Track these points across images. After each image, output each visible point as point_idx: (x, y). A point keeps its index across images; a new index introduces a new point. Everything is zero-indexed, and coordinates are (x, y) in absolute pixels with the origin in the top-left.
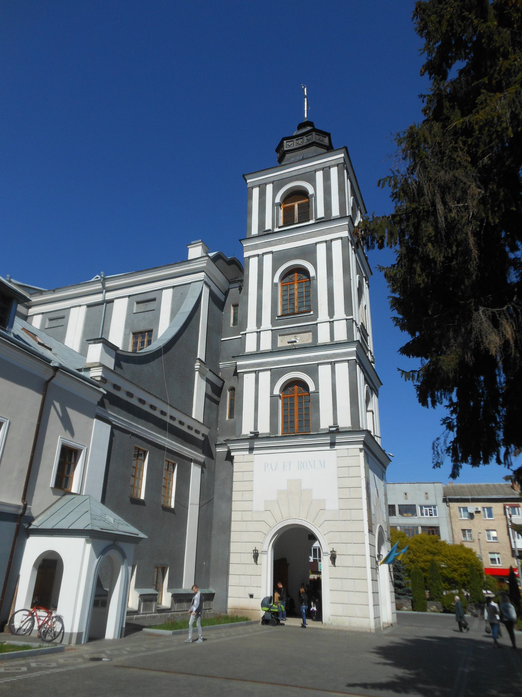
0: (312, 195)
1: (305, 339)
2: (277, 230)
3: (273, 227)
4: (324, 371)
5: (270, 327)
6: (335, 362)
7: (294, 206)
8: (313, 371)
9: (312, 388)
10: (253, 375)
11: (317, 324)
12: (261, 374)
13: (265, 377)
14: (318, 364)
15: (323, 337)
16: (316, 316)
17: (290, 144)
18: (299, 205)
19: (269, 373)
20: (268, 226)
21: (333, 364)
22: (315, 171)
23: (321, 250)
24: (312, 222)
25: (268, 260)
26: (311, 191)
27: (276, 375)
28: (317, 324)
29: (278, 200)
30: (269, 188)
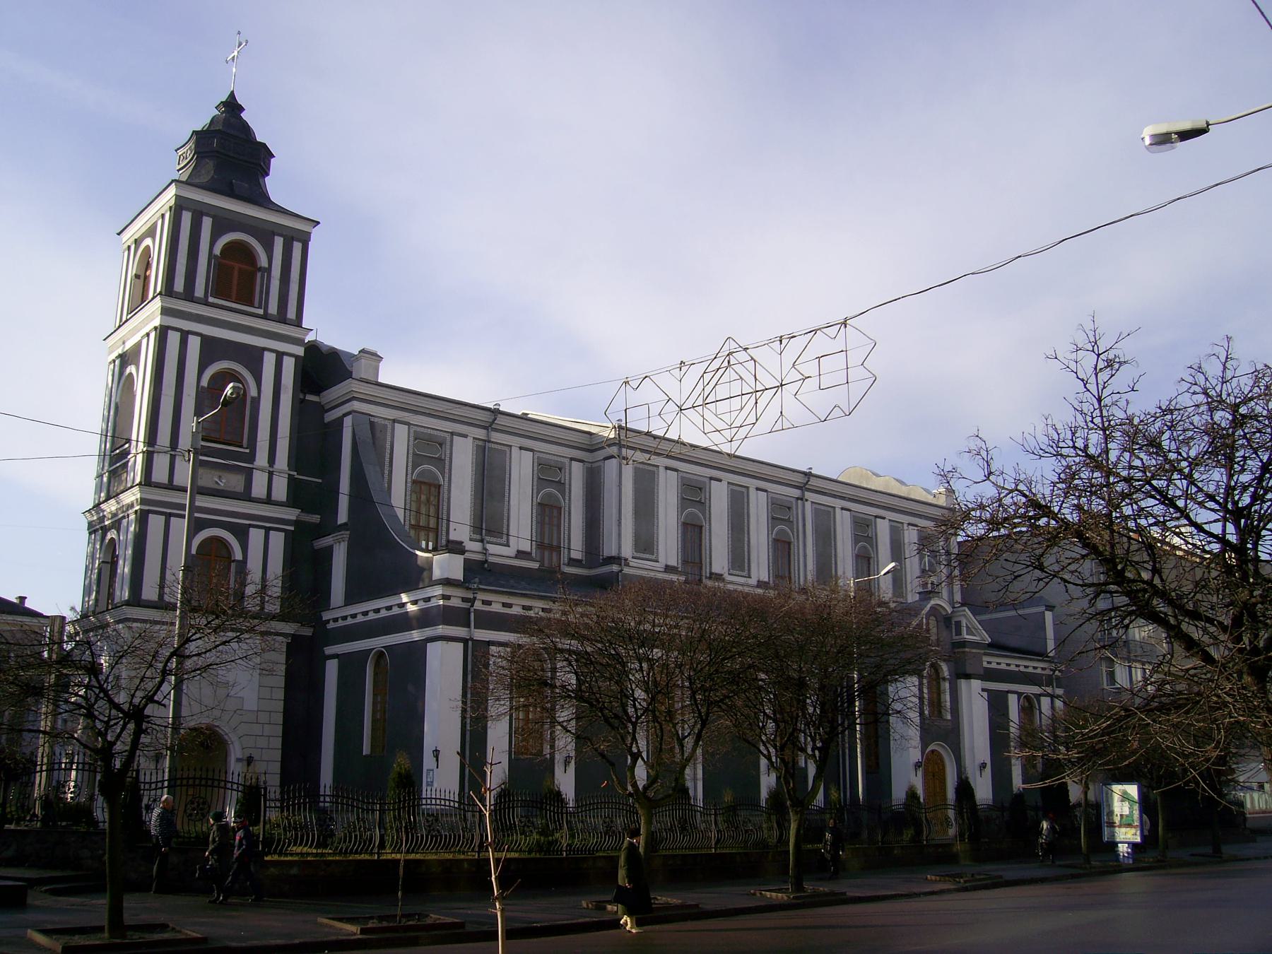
0: (264, 268)
1: (234, 482)
2: (211, 300)
4: (256, 536)
6: (271, 529)
8: (242, 533)
9: (238, 555)
10: (163, 518)
13: (181, 527)
14: (250, 526)
15: (259, 489)
16: (251, 457)
18: (240, 269)
20: (199, 291)
21: (268, 530)
22: (274, 234)
23: (269, 361)
24: (261, 312)
25: (194, 344)
26: (263, 262)
27: (196, 526)
29: (217, 250)
30: (207, 223)
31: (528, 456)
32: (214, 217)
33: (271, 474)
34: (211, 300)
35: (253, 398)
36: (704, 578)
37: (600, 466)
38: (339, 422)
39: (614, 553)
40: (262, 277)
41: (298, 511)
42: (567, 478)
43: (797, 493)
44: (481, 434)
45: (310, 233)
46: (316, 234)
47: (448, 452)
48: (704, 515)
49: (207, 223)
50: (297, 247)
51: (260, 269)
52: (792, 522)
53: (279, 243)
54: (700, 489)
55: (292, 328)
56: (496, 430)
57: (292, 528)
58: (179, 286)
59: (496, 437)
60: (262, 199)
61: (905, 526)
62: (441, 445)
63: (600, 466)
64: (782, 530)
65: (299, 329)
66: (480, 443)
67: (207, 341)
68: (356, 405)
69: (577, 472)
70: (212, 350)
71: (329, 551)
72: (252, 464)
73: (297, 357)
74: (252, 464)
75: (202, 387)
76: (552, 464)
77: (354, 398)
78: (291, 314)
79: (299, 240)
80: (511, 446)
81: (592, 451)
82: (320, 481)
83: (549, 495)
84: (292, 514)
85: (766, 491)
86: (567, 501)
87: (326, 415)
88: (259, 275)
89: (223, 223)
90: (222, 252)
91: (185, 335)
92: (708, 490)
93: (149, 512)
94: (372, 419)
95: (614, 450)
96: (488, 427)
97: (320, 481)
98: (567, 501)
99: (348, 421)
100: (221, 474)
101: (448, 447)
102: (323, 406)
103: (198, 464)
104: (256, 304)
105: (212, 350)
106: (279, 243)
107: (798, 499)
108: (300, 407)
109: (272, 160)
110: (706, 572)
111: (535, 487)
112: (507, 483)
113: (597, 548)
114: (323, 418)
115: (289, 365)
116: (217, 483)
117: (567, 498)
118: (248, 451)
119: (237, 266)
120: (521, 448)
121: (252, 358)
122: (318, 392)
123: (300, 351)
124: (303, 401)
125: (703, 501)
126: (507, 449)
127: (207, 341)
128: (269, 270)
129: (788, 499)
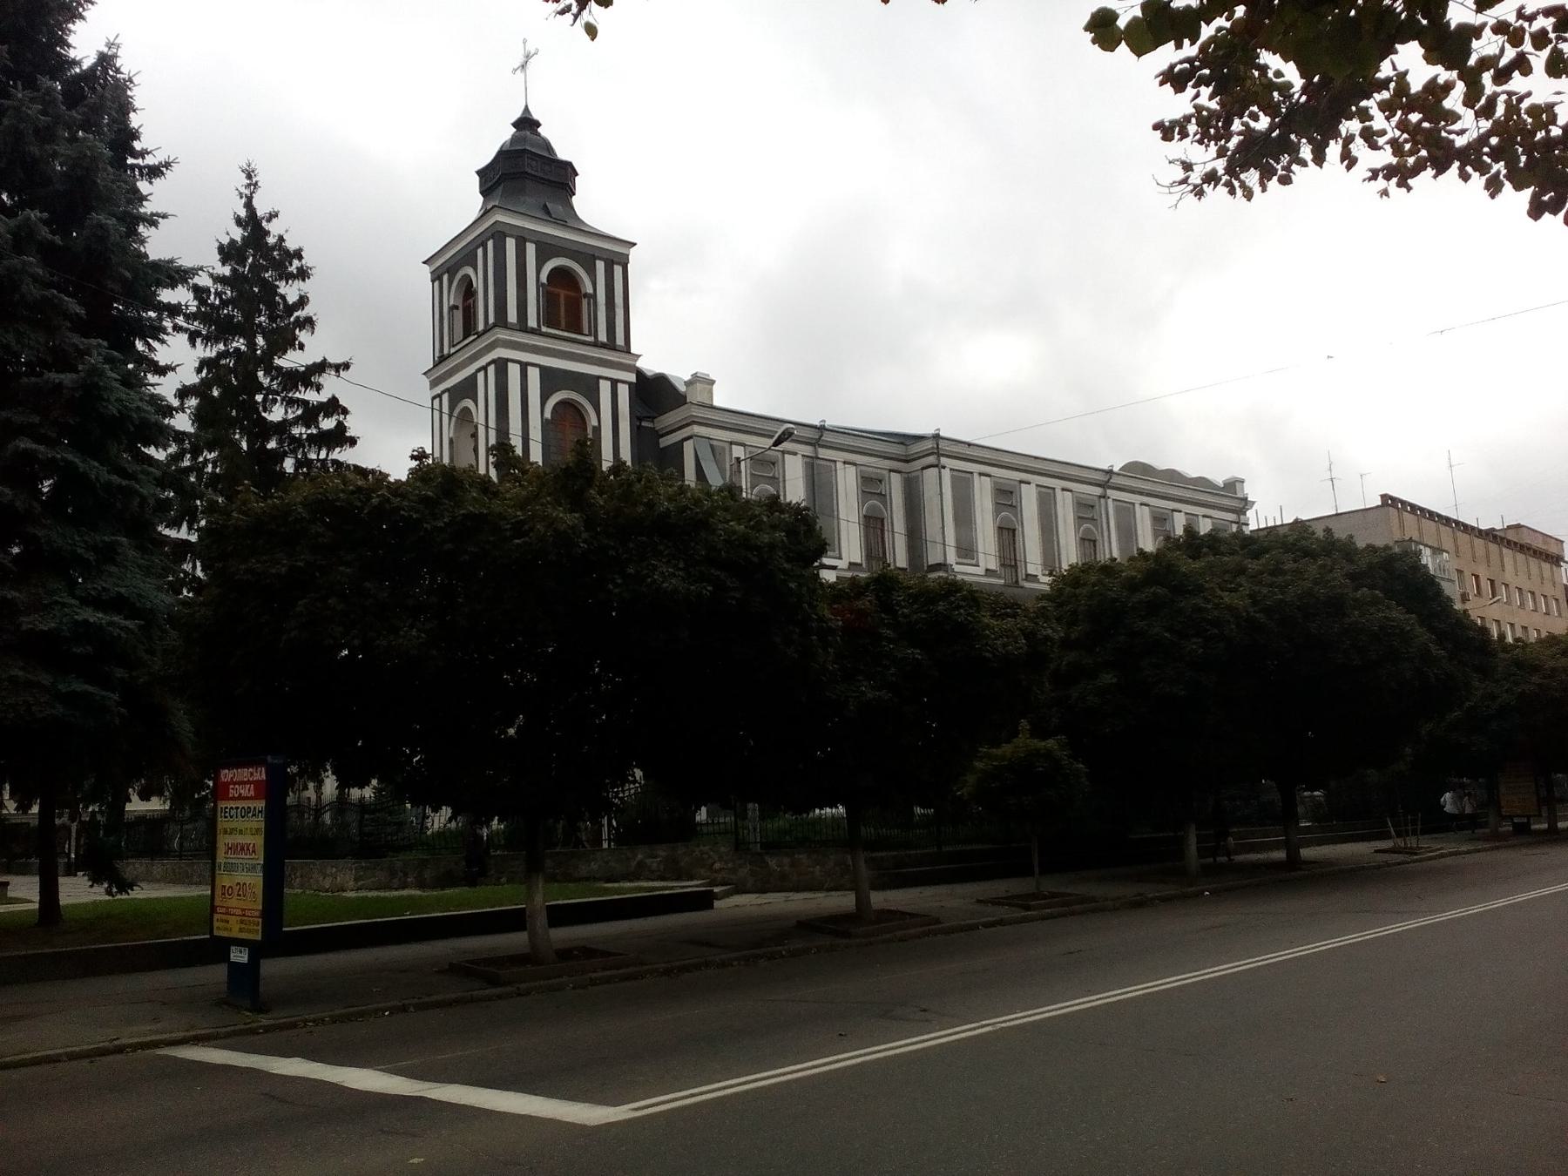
0: (589, 294)
2: (544, 329)
3: (539, 325)
7: (559, 295)
18: (567, 297)
23: (605, 387)
25: (534, 375)
29: (544, 278)
30: (531, 249)
31: (852, 469)
32: (536, 243)
34: (544, 329)
35: (594, 427)
36: (1020, 579)
37: (918, 477)
38: (679, 446)
39: (940, 560)
40: (589, 304)
42: (888, 490)
43: (1098, 491)
44: (808, 450)
45: (628, 255)
46: (633, 254)
47: (781, 471)
48: (1016, 516)
49: (531, 249)
50: (618, 270)
51: (586, 295)
52: (1096, 520)
53: (600, 265)
54: (1011, 493)
55: (623, 355)
56: (823, 446)
58: (512, 317)
59: (824, 453)
60: (569, 219)
61: (1137, 506)
62: (774, 464)
63: (918, 477)
64: (1089, 529)
65: (627, 356)
66: (808, 460)
67: (546, 372)
68: (697, 429)
69: (896, 482)
70: (552, 379)
73: (630, 384)
75: (547, 420)
76: (873, 476)
77: (694, 423)
79: (619, 264)
80: (835, 461)
81: (907, 461)
83: (873, 507)
85: (1071, 491)
86: (889, 512)
87: (661, 440)
88: (585, 302)
89: (547, 249)
90: (548, 281)
91: (524, 367)
92: (1018, 493)
94: (711, 442)
95: (931, 459)
96: (816, 443)
98: (889, 512)
99: (688, 447)
101: (781, 466)
102: (657, 431)
104: (586, 331)
105: (552, 379)
106: (600, 265)
107: (1100, 497)
108: (637, 432)
109: (577, 178)
110: (1022, 575)
111: (860, 501)
112: (835, 495)
113: (921, 557)
115: (624, 392)
117: (889, 509)
120: (845, 463)
121: (589, 386)
122: (652, 419)
123: (632, 378)
124: (639, 427)
125: (1014, 504)
126: (832, 465)
127: (546, 372)
128: (594, 296)
129: (1091, 497)
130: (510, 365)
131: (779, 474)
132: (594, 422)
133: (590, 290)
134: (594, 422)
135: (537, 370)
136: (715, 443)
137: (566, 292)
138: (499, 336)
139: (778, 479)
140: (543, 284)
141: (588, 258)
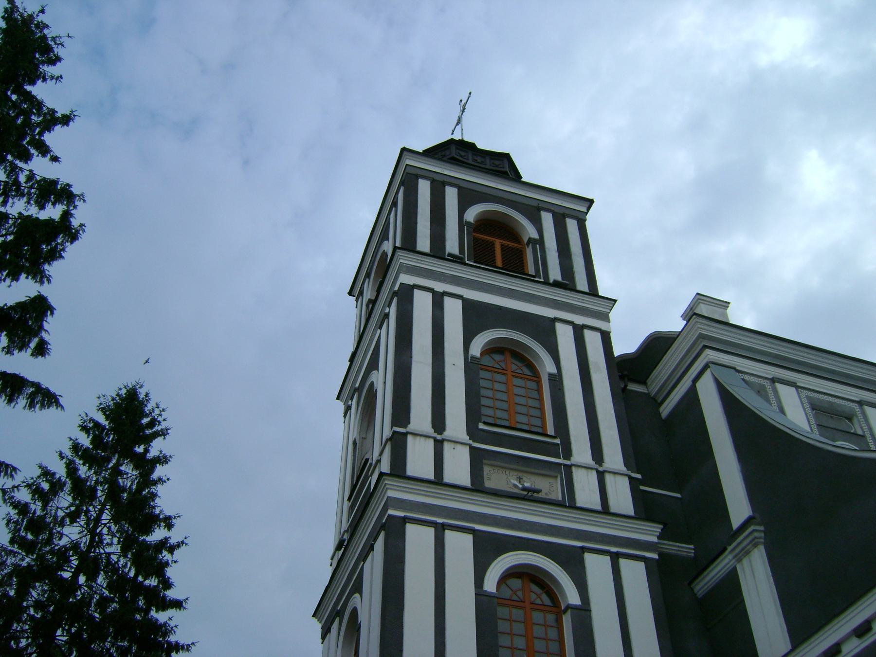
5: (465, 438)
7: (493, 244)
9: (573, 597)
11: (569, 468)
12: (448, 534)
14: (583, 549)
17: (463, 153)
18: (503, 247)
19: (468, 539)
24: (542, 280)
25: (453, 311)
26: (531, 232)
28: (569, 468)
32: (460, 188)
33: (601, 476)
35: (550, 375)
41: (657, 528)
51: (531, 241)
57: (655, 556)
67: (470, 309)
71: (732, 582)
72: (569, 460)
74: (569, 460)
75: (473, 357)
78: (582, 284)
82: (679, 495)
84: (649, 533)
87: (661, 409)
88: (529, 252)
91: (438, 300)
93: (405, 520)
97: (679, 495)
100: (520, 474)
102: (654, 399)
103: (477, 459)
114: (660, 414)
116: (515, 486)
118: (558, 441)
119: (498, 243)
128: (541, 241)
130: (417, 293)
131: (862, 429)
132: (553, 370)
133: (534, 234)
134: (553, 370)
135: (459, 303)
136: (747, 377)
137: (501, 241)
138: (401, 261)
139: (863, 436)
140: (468, 223)
141: (533, 212)
